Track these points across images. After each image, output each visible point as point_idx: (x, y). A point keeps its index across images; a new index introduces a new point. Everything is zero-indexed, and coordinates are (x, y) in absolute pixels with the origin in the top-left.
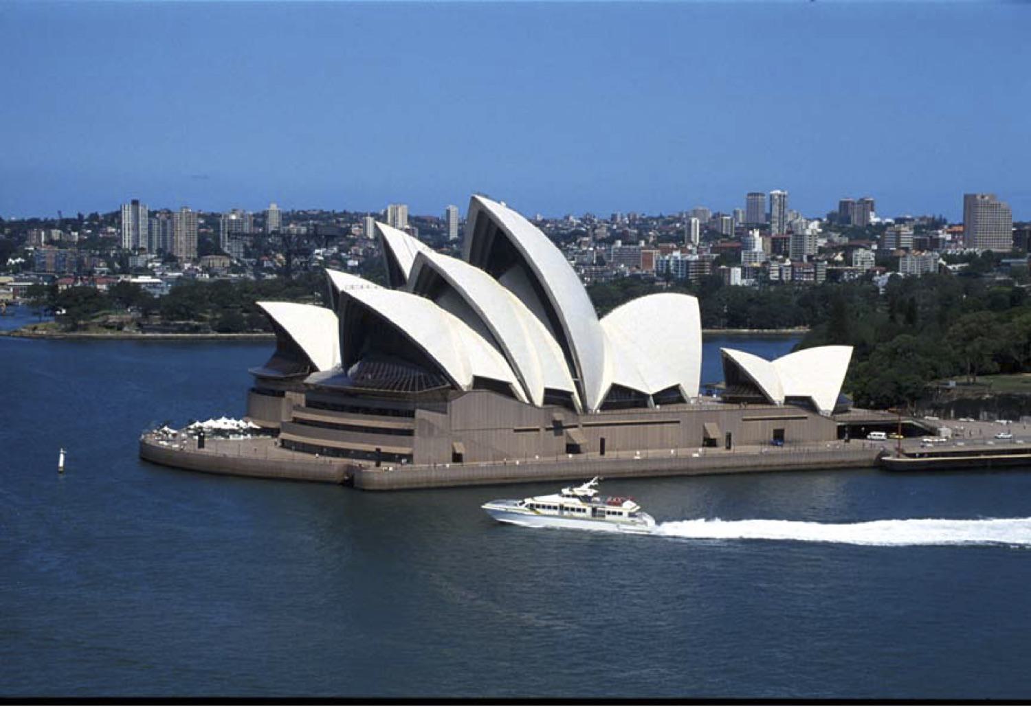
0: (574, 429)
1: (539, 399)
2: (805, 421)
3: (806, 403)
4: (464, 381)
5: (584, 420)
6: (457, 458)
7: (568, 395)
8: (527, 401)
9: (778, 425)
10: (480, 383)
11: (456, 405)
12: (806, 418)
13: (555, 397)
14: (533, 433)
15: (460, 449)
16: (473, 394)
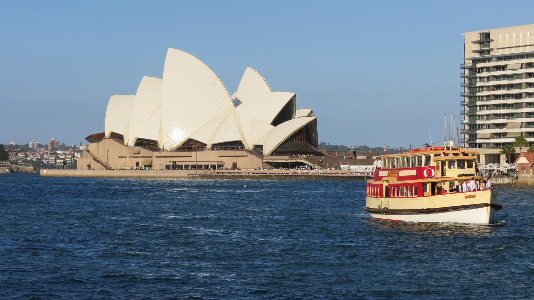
5: (156, 154)
7: (156, 142)
14: (124, 158)
15: (88, 164)
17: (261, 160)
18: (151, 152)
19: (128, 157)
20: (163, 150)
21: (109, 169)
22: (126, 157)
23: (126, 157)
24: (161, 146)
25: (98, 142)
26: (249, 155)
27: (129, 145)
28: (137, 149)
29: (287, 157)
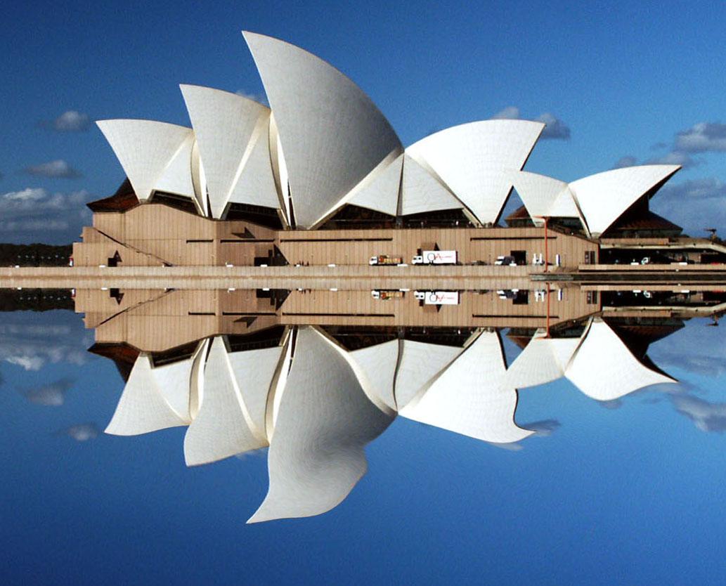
0: (267, 243)
1: (218, 212)
2: (554, 241)
3: (571, 226)
4: (143, 192)
5: (281, 235)
6: (113, 262)
7: (274, 210)
8: (207, 215)
9: (518, 246)
10: (159, 198)
11: (131, 214)
12: (555, 238)
13: (236, 212)
14: (206, 244)
16: (145, 206)
17: (597, 246)
18: (270, 231)
19: (215, 241)
20: (293, 227)
21: (486, 264)
22: (212, 241)
23: (212, 241)
24: (287, 220)
25: (123, 210)
26: (559, 235)
27: (214, 217)
28: (239, 226)
29: (666, 240)
